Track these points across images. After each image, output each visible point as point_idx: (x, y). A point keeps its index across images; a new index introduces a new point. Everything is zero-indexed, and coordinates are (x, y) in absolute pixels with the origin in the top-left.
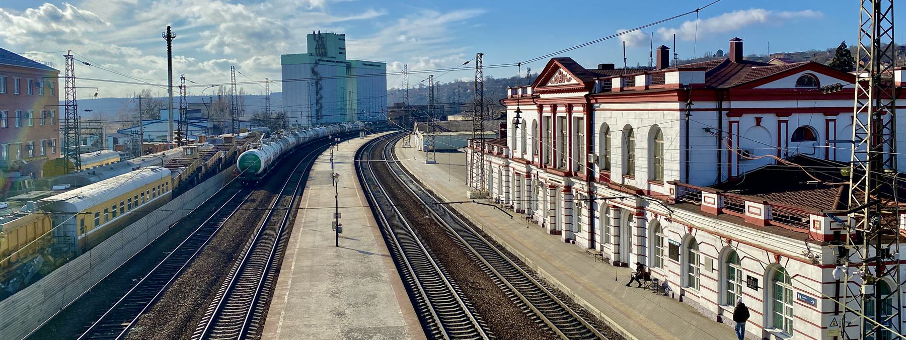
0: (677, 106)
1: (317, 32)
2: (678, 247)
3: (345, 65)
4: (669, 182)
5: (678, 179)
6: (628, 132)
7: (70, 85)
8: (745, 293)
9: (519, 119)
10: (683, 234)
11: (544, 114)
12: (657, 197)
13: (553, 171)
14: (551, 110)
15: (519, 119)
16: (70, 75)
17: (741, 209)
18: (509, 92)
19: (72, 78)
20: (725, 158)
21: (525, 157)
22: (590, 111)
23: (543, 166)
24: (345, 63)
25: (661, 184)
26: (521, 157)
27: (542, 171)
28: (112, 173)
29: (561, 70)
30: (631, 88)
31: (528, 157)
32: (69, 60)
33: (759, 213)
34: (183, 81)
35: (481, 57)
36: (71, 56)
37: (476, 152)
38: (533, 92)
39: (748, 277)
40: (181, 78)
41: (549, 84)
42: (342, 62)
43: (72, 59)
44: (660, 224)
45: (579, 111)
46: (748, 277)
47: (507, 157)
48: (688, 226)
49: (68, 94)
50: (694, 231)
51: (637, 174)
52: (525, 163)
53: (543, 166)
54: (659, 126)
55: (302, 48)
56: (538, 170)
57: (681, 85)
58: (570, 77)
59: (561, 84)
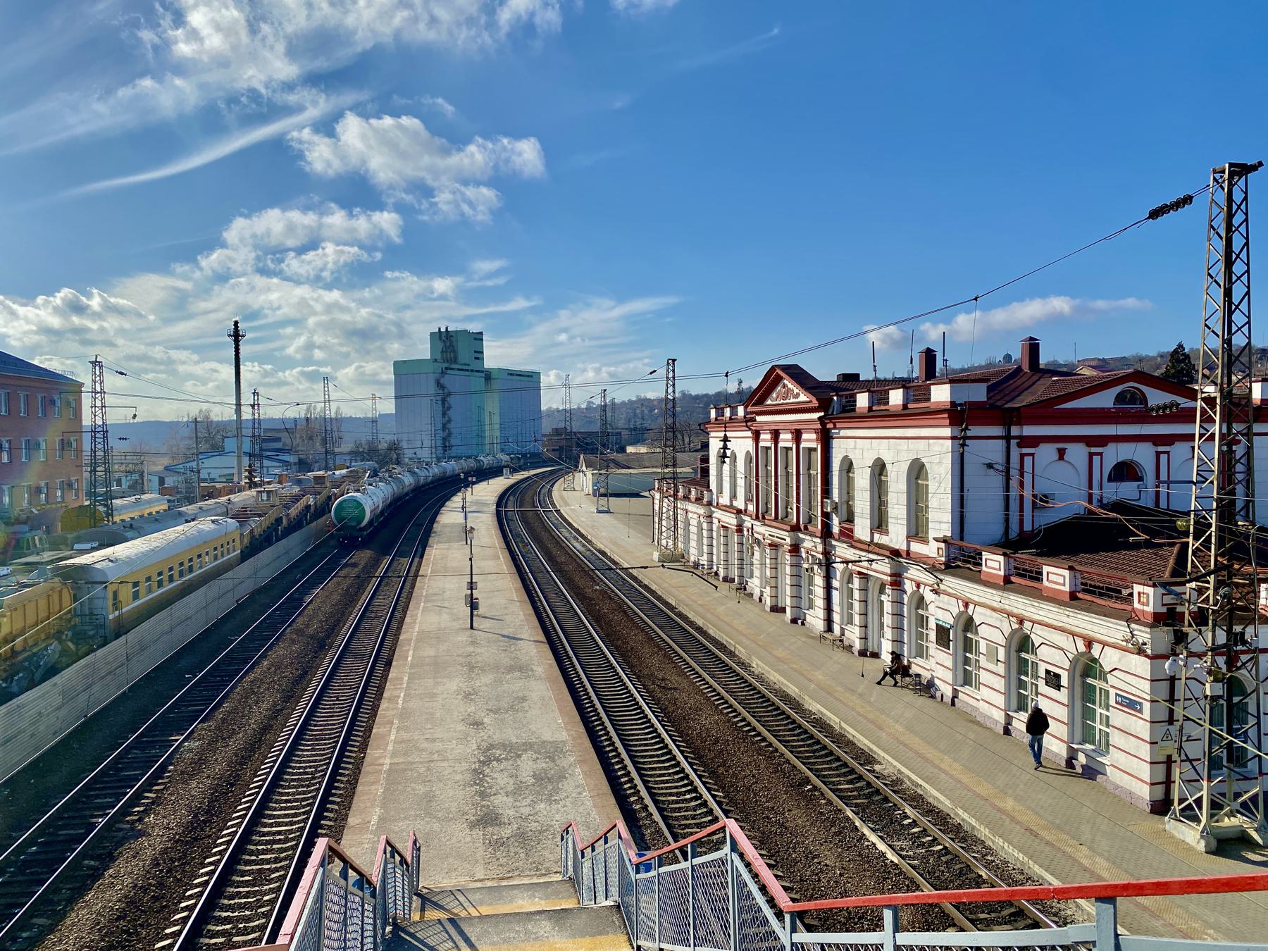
0: (947, 432)
1: (443, 330)
4: (936, 539)
5: (949, 534)
6: (879, 469)
7: (99, 404)
8: (1042, 695)
10: (955, 612)
11: (761, 444)
12: (920, 560)
13: (775, 524)
16: (98, 389)
17: (1037, 576)
18: (713, 413)
19: (101, 392)
20: (1014, 505)
21: (735, 503)
22: (826, 439)
24: (482, 372)
25: (926, 542)
27: (759, 524)
28: (157, 526)
29: (786, 382)
30: (883, 407)
31: (740, 503)
32: (97, 368)
33: (1062, 581)
35: (674, 364)
36: (99, 362)
38: (746, 413)
39: (1048, 672)
40: (254, 393)
41: (769, 402)
42: (478, 371)
43: (101, 367)
45: (810, 440)
46: (1048, 672)
47: (710, 504)
48: (963, 601)
49: (95, 416)
50: (971, 607)
51: (891, 527)
54: (923, 460)
55: (423, 351)
57: (953, 403)
59: (785, 402)
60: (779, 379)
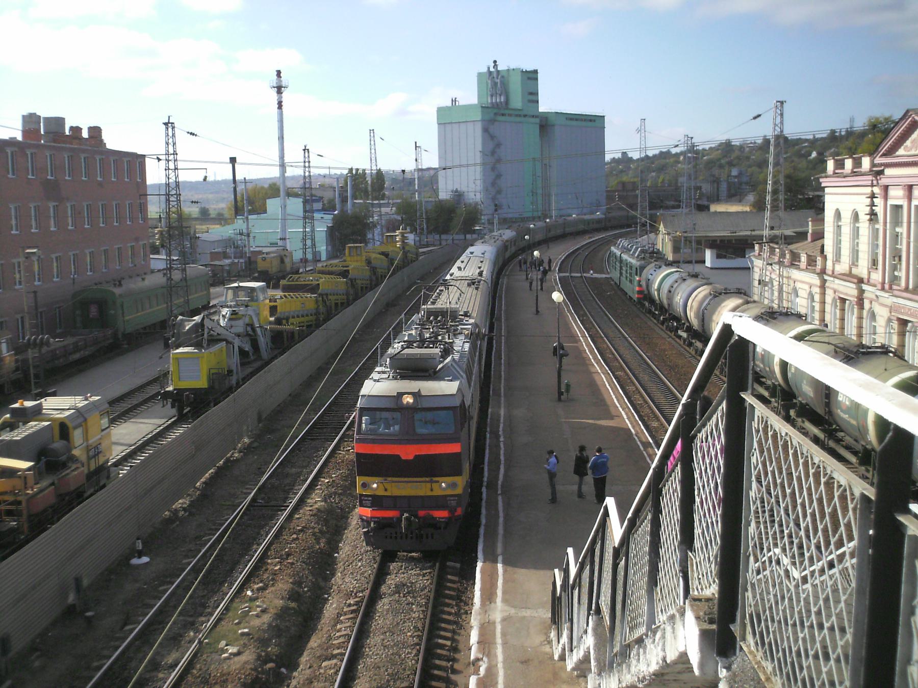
7: (172, 166)
11: (891, 202)
14: (904, 194)
16: (171, 151)
18: (830, 165)
19: (174, 154)
21: (854, 271)
23: (887, 286)
24: (537, 117)
26: (848, 272)
27: (886, 295)
31: (862, 269)
34: (170, 130)
36: (172, 123)
37: (771, 264)
38: (873, 165)
40: (304, 150)
43: (173, 128)
47: (823, 271)
49: (168, 178)
52: (856, 281)
53: (887, 286)
55: (469, 95)
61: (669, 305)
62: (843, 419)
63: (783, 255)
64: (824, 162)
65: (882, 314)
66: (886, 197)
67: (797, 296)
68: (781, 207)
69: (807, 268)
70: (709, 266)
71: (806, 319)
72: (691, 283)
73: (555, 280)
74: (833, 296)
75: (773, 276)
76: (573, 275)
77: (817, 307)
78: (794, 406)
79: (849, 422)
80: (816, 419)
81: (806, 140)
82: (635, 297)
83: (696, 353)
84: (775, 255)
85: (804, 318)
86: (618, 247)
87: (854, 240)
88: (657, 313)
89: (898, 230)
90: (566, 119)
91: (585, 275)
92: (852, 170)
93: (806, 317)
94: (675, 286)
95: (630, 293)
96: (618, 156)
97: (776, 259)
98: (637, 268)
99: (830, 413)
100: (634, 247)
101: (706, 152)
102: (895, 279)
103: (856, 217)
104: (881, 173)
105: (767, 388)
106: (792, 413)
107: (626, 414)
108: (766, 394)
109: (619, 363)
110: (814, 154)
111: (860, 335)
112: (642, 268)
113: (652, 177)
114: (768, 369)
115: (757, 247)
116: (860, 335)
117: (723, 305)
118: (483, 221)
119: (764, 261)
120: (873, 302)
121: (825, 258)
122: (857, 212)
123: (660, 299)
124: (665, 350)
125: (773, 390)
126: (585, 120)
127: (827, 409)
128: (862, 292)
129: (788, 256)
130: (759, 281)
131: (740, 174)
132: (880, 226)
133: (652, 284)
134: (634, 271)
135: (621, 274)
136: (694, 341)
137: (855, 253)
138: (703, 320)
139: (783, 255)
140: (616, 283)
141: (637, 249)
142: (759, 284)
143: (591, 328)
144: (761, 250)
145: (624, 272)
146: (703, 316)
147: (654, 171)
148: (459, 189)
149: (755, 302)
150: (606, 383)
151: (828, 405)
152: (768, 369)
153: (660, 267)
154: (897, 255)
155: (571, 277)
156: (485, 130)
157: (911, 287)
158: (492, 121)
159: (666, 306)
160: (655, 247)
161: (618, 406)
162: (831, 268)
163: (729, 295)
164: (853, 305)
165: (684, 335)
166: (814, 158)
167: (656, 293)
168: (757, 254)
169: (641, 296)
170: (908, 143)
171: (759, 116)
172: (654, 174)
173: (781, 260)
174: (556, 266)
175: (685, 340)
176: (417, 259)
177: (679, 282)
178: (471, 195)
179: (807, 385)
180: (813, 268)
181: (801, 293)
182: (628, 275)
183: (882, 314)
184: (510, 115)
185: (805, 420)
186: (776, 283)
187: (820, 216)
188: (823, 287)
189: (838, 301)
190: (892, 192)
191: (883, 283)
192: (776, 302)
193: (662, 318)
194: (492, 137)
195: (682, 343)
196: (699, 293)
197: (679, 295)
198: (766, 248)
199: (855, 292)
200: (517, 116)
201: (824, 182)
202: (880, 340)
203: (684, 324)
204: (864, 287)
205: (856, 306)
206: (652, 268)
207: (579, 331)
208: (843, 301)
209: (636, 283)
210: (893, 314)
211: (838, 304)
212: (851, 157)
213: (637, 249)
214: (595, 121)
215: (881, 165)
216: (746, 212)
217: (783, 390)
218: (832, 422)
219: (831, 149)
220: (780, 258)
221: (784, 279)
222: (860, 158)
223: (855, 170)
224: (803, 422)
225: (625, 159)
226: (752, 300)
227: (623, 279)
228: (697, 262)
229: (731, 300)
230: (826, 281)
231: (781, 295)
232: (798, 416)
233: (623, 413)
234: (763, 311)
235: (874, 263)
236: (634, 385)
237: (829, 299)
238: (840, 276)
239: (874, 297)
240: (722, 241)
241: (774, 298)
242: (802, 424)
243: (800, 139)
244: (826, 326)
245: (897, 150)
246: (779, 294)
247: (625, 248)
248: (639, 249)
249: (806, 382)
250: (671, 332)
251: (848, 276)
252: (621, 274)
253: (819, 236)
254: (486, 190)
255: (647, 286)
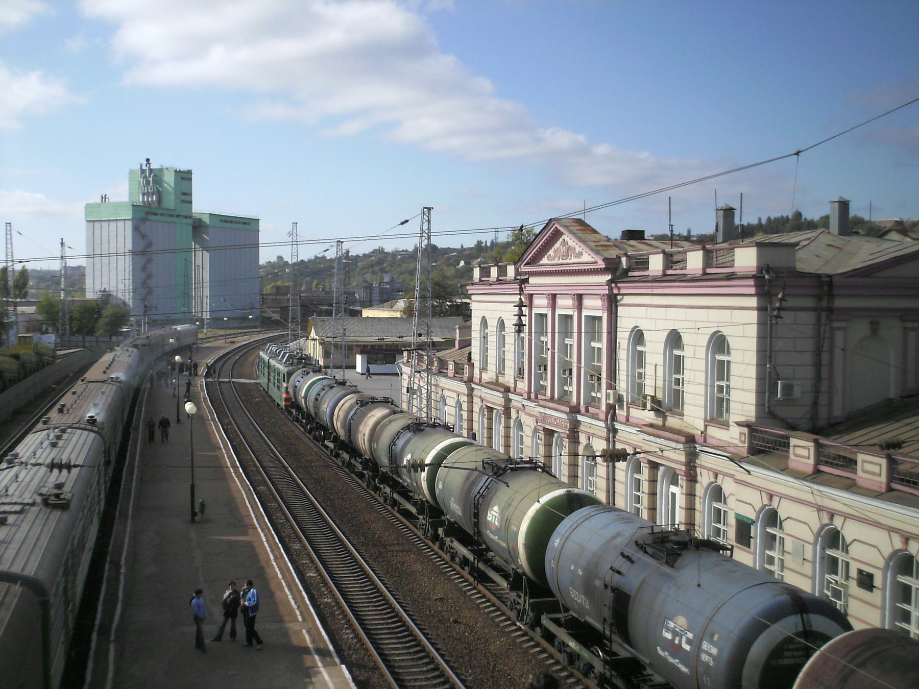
2: (750, 525)
3: (191, 221)
4: (739, 424)
5: (753, 420)
6: (675, 339)
9: (523, 318)
10: (758, 506)
15: (523, 318)
17: (850, 463)
18: (476, 273)
21: (501, 380)
22: (612, 303)
23: (533, 396)
25: (725, 425)
26: (495, 381)
27: (533, 405)
29: (567, 239)
31: (508, 378)
35: (429, 213)
37: (419, 372)
38: (517, 273)
39: (860, 572)
41: (544, 261)
42: (186, 217)
44: (721, 489)
45: (595, 307)
46: (860, 572)
47: (471, 380)
51: (687, 410)
52: (503, 390)
53: (533, 396)
56: (525, 403)
58: (581, 250)
59: (565, 262)
60: (557, 234)
61: (316, 413)
62: (492, 540)
63: (431, 363)
64: (471, 270)
65: (529, 423)
66: (531, 307)
67: (446, 405)
68: (429, 314)
69: (454, 376)
70: (360, 371)
71: (453, 431)
72: (337, 391)
73: (201, 386)
74: (480, 405)
75: (422, 384)
76: (221, 380)
77: (465, 415)
78: (442, 524)
79: (499, 544)
80: (466, 539)
81: (455, 250)
82: (283, 404)
83: (343, 464)
84: (422, 362)
85: (452, 430)
86: (267, 352)
87: (500, 349)
88: (304, 421)
89: (542, 339)
90: (220, 221)
91: (233, 380)
92: (498, 278)
93: (454, 428)
94: (322, 394)
95: (277, 400)
96: (273, 259)
97: (425, 367)
98: (284, 375)
99: (479, 533)
100: (283, 352)
101: (360, 259)
102: (541, 389)
103: (501, 324)
104: (526, 281)
105: (415, 504)
106: (440, 531)
107: (265, 535)
108: (413, 510)
109: (262, 476)
110: (462, 263)
111: (507, 446)
112: (290, 374)
113: (307, 282)
114: (415, 484)
115: (405, 354)
116: (507, 446)
117: (369, 415)
118: (131, 323)
119: (412, 368)
120: (520, 412)
121: (472, 366)
122: (503, 320)
123: (307, 407)
124: (311, 462)
125: (421, 506)
126: (239, 223)
127: (476, 529)
128: (508, 401)
129: (435, 364)
130: (408, 388)
131: (392, 281)
132: (525, 335)
133: (299, 391)
134: (281, 377)
135: (269, 380)
136: (341, 452)
137: (502, 362)
138: (350, 431)
139: (431, 363)
140: (264, 390)
141: (285, 354)
142: (408, 392)
143: (235, 438)
144: (409, 358)
145: (272, 378)
146: (350, 426)
147: (308, 276)
148: (107, 290)
149: (402, 412)
150: (246, 500)
151: (476, 525)
152: (415, 484)
153: (307, 374)
154: (542, 365)
155: (220, 382)
156: (136, 229)
157: (556, 397)
158: (144, 220)
159: (313, 415)
160: (303, 353)
161: (258, 526)
162: (478, 377)
163: (378, 403)
164: (501, 414)
165: (331, 445)
166: (462, 267)
167: (303, 400)
168: (406, 362)
169: (289, 403)
170: (551, 252)
171: (407, 221)
172: (308, 279)
173: (429, 367)
174: (202, 370)
175: (332, 451)
176: (54, 362)
177: (327, 389)
178: (120, 296)
179: (454, 503)
180: (461, 376)
181: (449, 401)
182: (276, 382)
183: (529, 423)
184: (163, 215)
185: (453, 539)
186: (424, 391)
187: (468, 323)
188: (470, 395)
189: (486, 410)
190: (537, 301)
191: (529, 393)
192: (425, 410)
193: (309, 427)
194: (143, 236)
195: (329, 453)
196: (346, 402)
197: (326, 403)
198: (415, 355)
199: (501, 401)
200: (169, 215)
201: (471, 290)
202: (527, 454)
203: (332, 433)
204: (511, 396)
205: (503, 416)
206: (300, 374)
207: (222, 441)
208: (490, 410)
209: (283, 390)
210: (539, 424)
211: (486, 413)
212: (496, 265)
213: (285, 354)
214: (249, 224)
215: (526, 273)
216: (397, 318)
217: (430, 506)
218: (481, 541)
219: (477, 259)
220: (428, 366)
221: (433, 387)
222: (506, 266)
223: (500, 278)
224: (452, 542)
225: (281, 263)
226: (399, 410)
227: (271, 385)
228: (348, 367)
229: (376, 410)
230: (473, 389)
231: (429, 403)
232: (447, 535)
233: (262, 535)
234: (410, 422)
235: (520, 371)
236: (277, 501)
237: (476, 408)
238: (486, 385)
239: (521, 406)
240: (372, 346)
241: (423, 406)
242: (450, 544)
243: (449, 248)
244: (474, 437)
245: (541, 259)
246: (428, 402)
247: (273, 353)
248: (287, 354)
249: (455, 499)
250: (318, 441)
251: (495, 385)
252: (269, 380)
253: (466, 343)
254: (135, 290)
255: (295, 393)
